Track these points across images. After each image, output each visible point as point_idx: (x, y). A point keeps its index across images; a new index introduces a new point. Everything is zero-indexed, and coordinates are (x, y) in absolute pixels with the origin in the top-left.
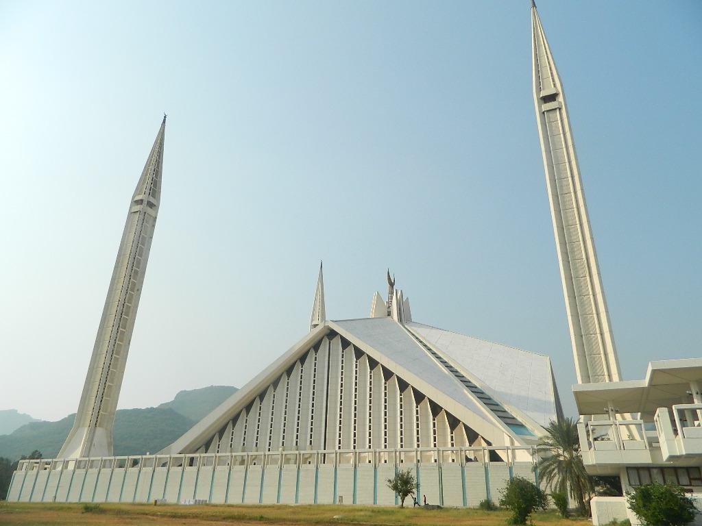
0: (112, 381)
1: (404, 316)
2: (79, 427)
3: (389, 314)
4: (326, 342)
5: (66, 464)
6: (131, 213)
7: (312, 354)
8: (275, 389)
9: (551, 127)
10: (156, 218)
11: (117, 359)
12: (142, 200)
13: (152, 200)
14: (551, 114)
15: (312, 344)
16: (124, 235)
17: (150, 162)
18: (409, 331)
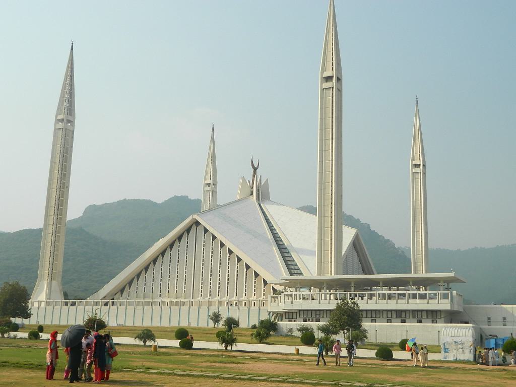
0: (58, 250)
1: (262, 195)
2: (41, 280)
3: (252, 194)
4: (194, 227)
5: (40, 303)
6: (56, 130)
7: (185, 236)
8: (163, 257)
9: (326, 101)
10: (73, 131)
11: (59, 236)
12: (63, 120)
13: (70, 118)
14: (327, 91)
15: (186, 228)
16: (53, 146)
17: (65, 87)
18: (262, 209)
